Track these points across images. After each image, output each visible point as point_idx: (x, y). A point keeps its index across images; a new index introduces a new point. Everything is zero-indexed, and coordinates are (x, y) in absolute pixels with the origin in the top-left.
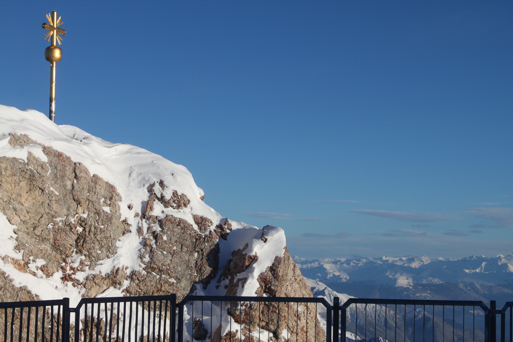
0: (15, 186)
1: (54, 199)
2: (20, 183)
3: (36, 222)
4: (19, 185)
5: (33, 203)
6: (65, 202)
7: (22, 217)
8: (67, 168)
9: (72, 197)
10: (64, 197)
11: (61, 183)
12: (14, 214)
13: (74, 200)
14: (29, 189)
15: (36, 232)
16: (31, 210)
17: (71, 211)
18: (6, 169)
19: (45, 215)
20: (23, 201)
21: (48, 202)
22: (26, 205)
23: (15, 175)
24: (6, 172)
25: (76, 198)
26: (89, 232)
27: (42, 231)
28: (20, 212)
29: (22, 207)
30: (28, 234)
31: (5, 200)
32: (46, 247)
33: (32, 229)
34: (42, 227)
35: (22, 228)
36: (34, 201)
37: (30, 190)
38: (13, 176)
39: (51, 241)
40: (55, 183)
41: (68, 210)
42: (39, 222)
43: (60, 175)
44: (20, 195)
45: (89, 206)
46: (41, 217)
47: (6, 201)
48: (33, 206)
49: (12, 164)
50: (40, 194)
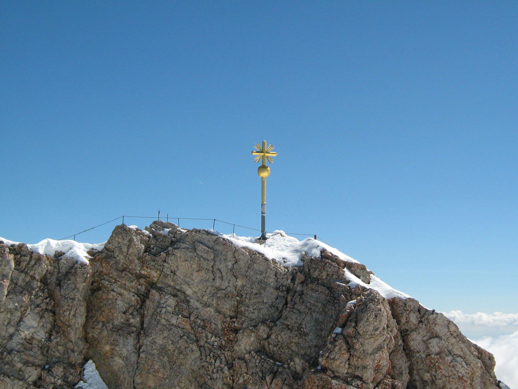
0: (189, 268)
1: (218, 275)
2: (192, 266)
3: (204, 292)
4: (191, 267)
5: (201, 279)
6: (227, 277)
7: (194, 289)
8: (229, 253)
9: (232, 273)
10: (226, 274)
11: (224, 264)
12: (188, 287)
13: (235, 276)
14: (198, 269)
15: (203, 299)
16: (199, 284)
17: (231, 283)
18: (180, 257)
19: (210, 289)
20: (194, 278)
21: (213, 277)
22: (196, 281)
23: (187, 261)
24: (180, 259)
25: (235, 274)
26: (246, 297)
27: (208, 298)
28: (192, 286)
29: (194, 282)
30: (198, 301)
31: (182, 278)
32: (211, 309)
33: (201, 297)
34: (207, 296)
35: (194, 297)
36: (202, 278)
37: (199, 270)
38: (185, 261)
39: (215, 305)
40: (221, 264)
41: (229, 283)
42: (205, 293)
43: (224, 259)
44: (192, 274)
45: (247, 279)
46: (206, 289)
47: (183, 279)
48: (201, 281)
49: (184, 253)
50: (206, 272)
